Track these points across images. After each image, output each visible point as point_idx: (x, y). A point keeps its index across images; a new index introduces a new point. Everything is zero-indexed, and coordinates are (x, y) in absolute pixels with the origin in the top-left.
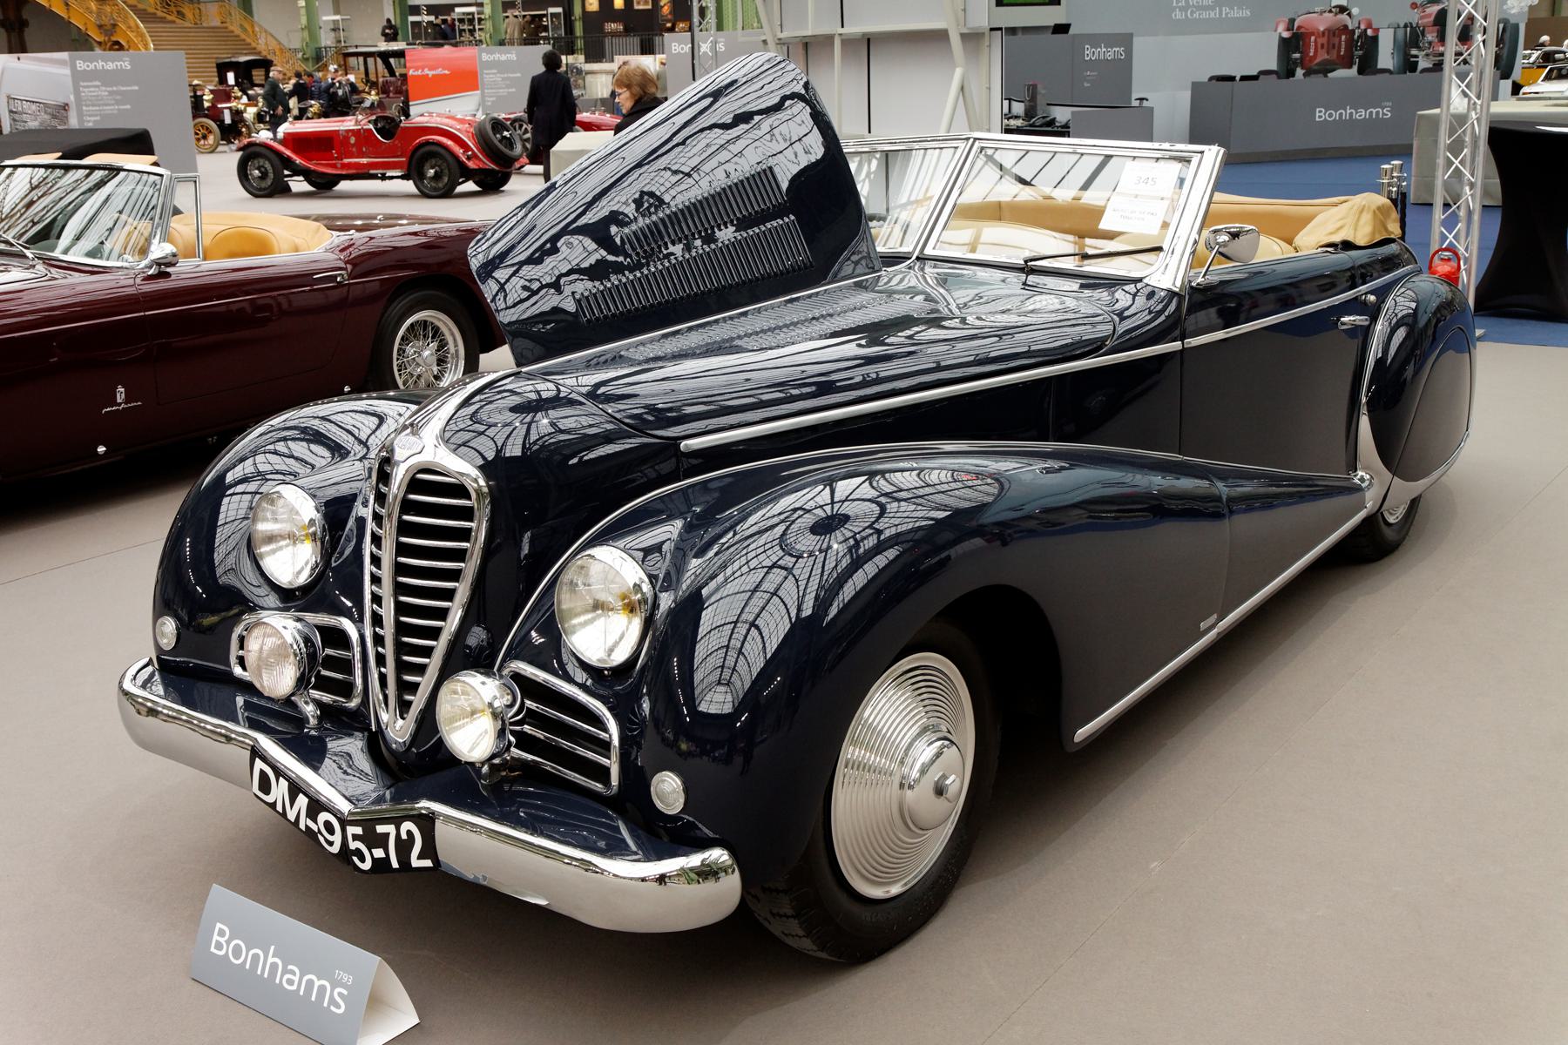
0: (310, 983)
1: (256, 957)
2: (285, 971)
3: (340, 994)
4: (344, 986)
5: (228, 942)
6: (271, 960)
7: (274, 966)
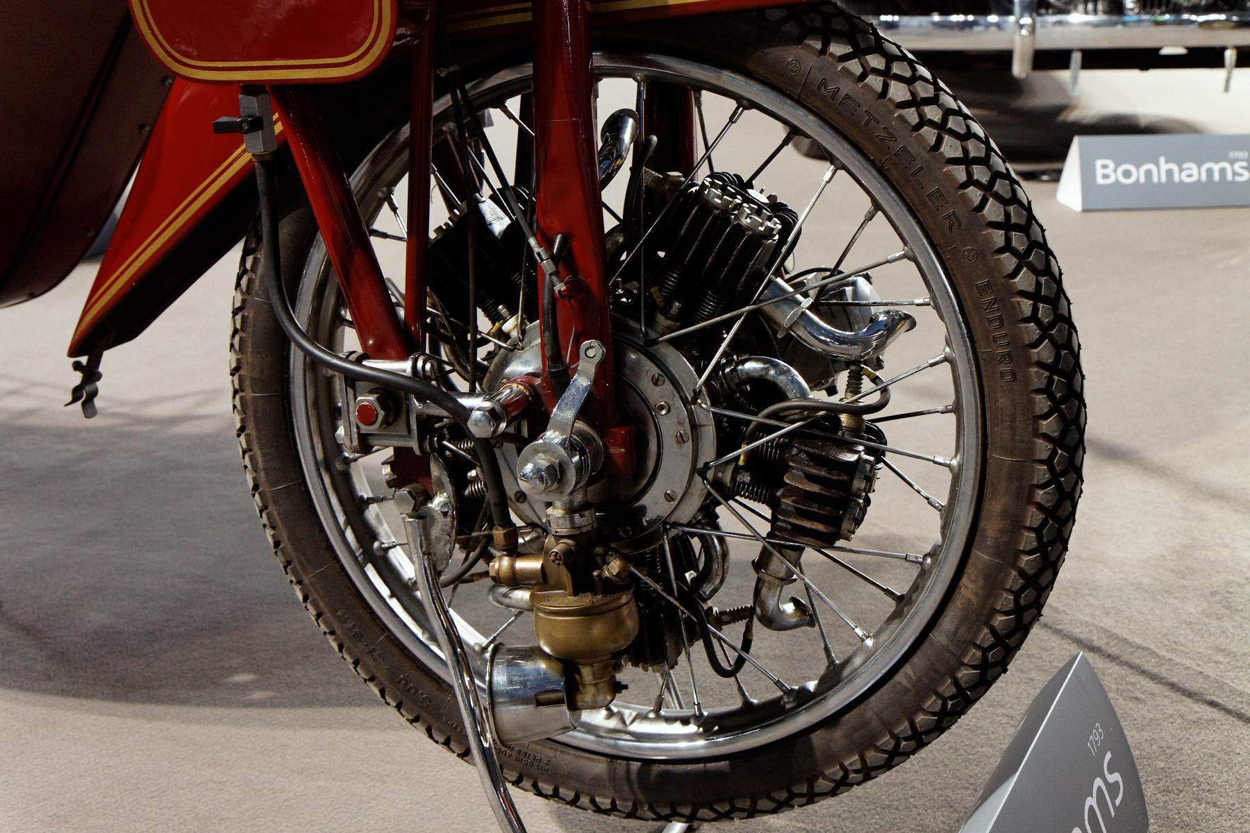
0: (1210, 171)
1: (1148, 173)
2: (1181, 170)
4: (1242, 160)
5: (1115, 171)
6: (1164, 167)
7: (1170, 173)
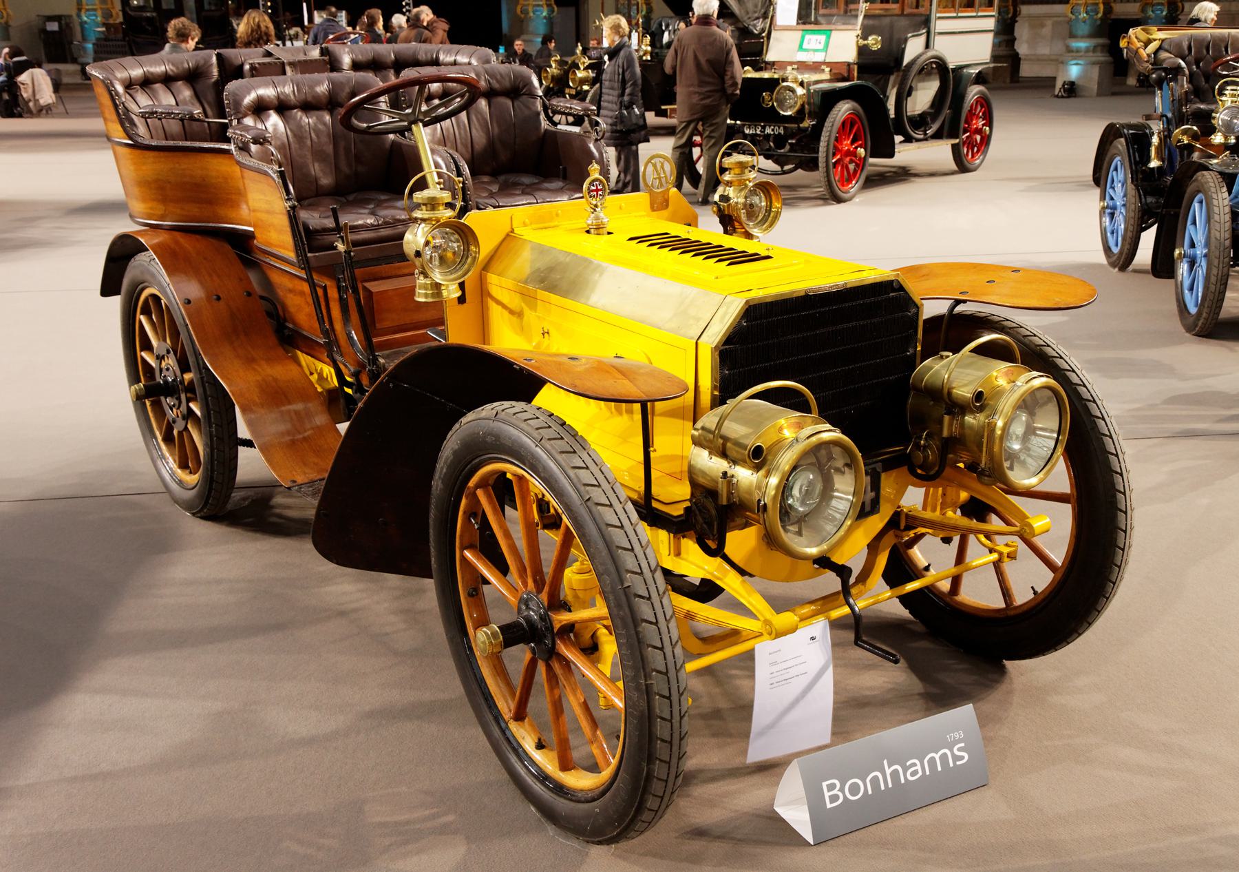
0: (932, 761)
1: (875, 781)
2: (905, 770)
3: (959, 750)
6: (888, 772)
7: (895, 774)
